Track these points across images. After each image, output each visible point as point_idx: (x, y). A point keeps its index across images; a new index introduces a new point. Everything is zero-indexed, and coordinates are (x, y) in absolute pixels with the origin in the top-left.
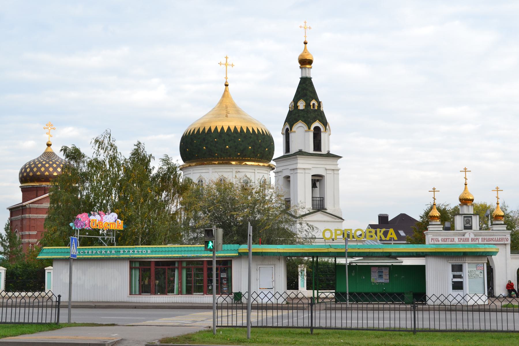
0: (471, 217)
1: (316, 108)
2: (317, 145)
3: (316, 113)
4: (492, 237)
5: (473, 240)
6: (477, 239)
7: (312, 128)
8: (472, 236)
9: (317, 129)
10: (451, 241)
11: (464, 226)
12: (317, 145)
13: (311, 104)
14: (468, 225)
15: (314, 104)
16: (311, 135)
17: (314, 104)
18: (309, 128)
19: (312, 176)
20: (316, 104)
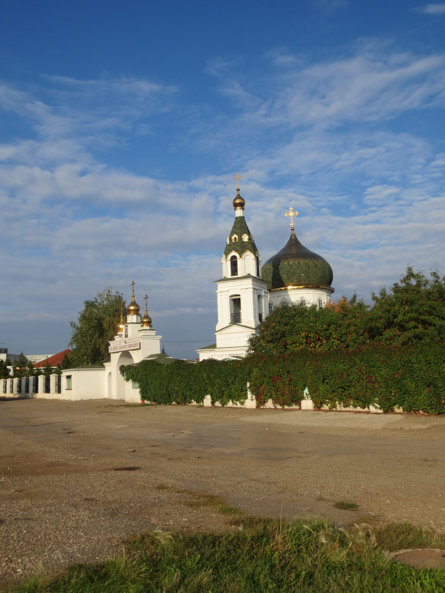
0: (127, 326)
1: (237, 241)
2: (234, 271)
3: (236, 245)
4: (131, 343)
5: (125, 346)
6: (126, 346)
7: (229, 257)
8: (124, 344)
9: (234, 258)
10: (117, 350)
11: (125, 335)
12: (234, 271)
13: (233, 238)
14: (126, 334)
15: (235, 238)
16: (229, 263)
17: (235, 238)
18: (226, 259)
19: (230, 296)
20: (237, 237)
